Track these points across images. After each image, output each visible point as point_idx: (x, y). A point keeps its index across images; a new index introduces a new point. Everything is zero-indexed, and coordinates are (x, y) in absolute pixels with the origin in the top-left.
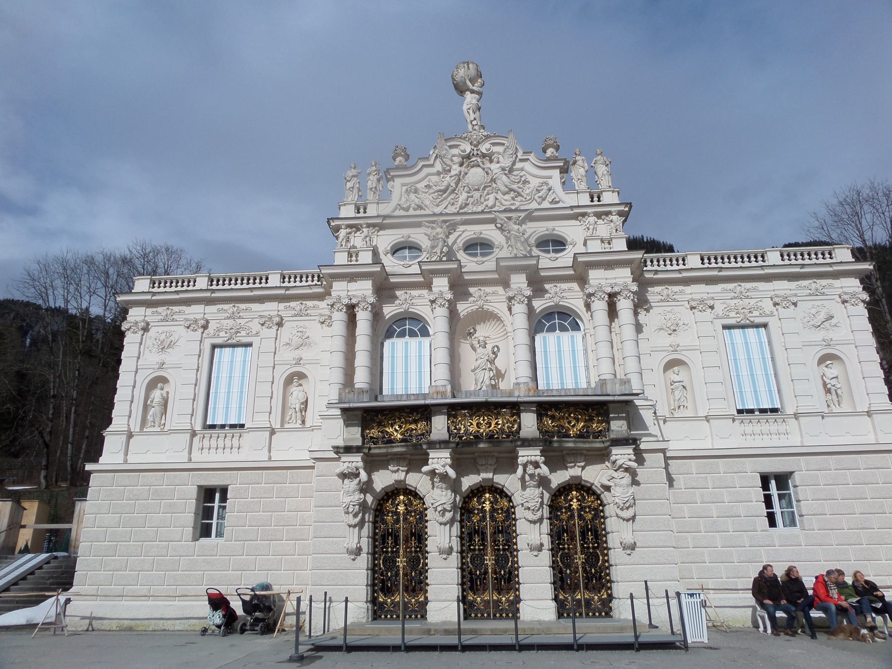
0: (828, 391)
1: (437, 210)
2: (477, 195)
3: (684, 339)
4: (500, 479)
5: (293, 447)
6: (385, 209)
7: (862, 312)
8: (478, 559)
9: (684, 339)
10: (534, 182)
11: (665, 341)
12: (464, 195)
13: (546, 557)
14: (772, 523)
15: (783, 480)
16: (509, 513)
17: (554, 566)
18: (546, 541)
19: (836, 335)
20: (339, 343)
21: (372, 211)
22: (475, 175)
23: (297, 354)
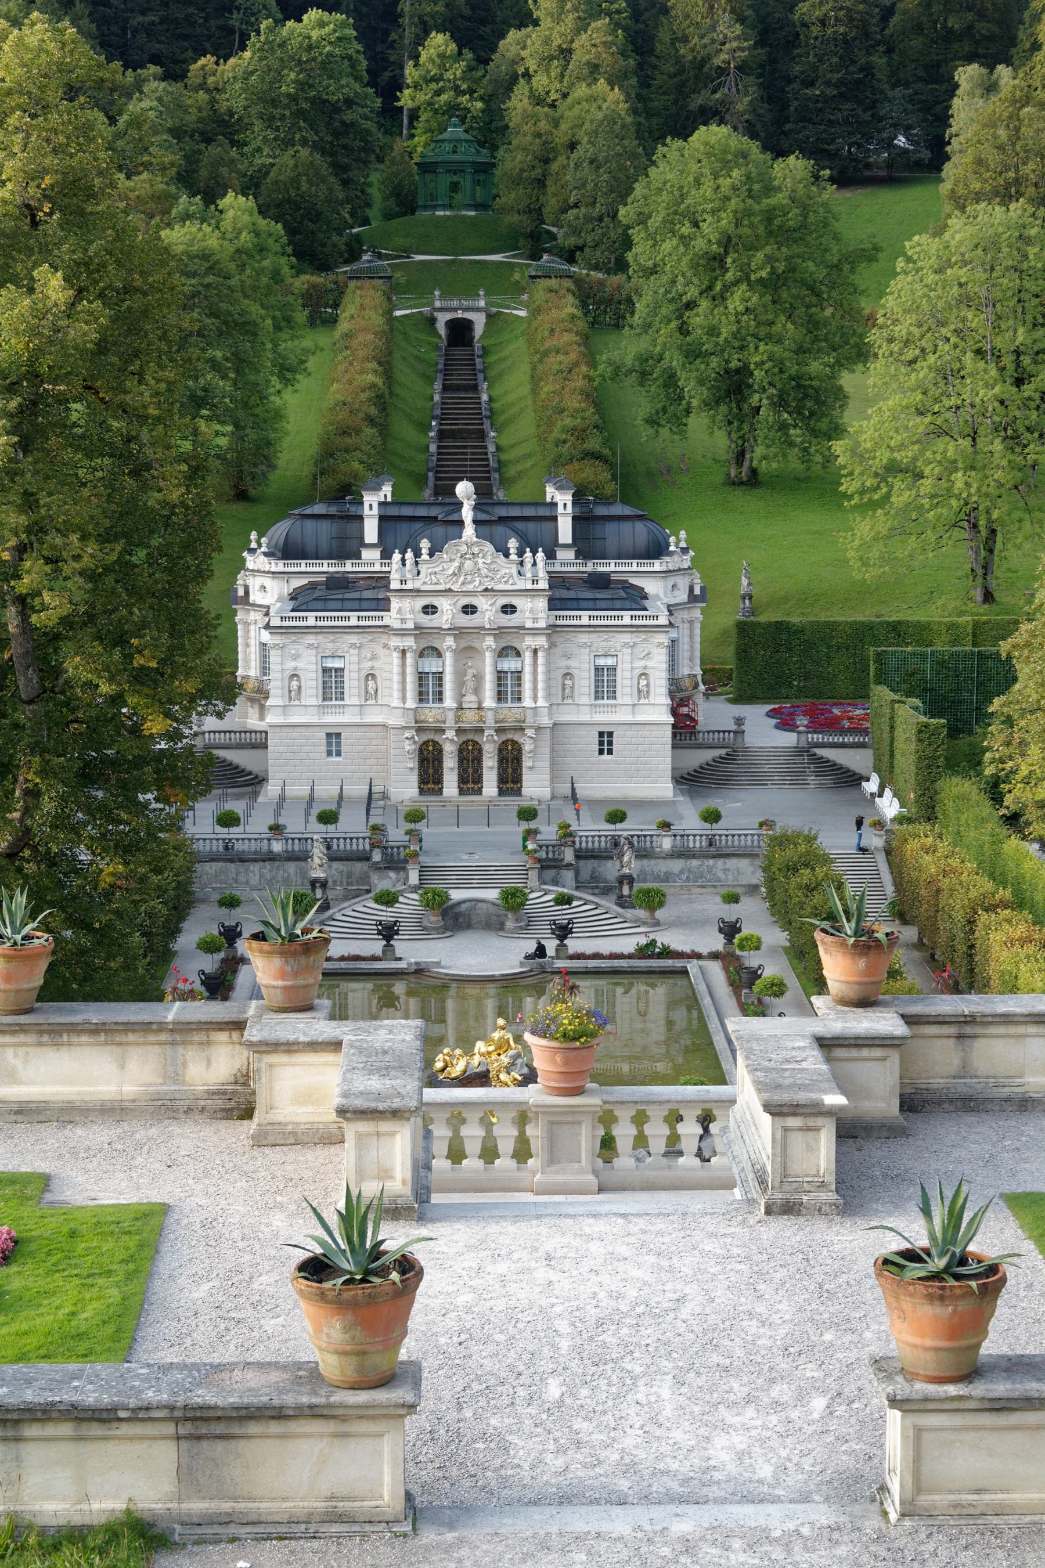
0: (639, 691)
1: (448, 586)
2: (469, 578)
3: (572, 663)
4: (476, 738)
5: (375, 717)
6: (418, 584)
7: (664, 651)
8: (465, 771)
9: (572, 663)
10: (502, 573)
11: (563, 663)
12: (462, 579)
13: (495, 772)
14: (601, 752)
15: (610, 734)
16: (480, 751)
17: (499, 774)
18: (496, 764)
19: (650, 664)
20: (396, 669)
21: (409, 586)
22: (468, 565)
23: (369, 664)
